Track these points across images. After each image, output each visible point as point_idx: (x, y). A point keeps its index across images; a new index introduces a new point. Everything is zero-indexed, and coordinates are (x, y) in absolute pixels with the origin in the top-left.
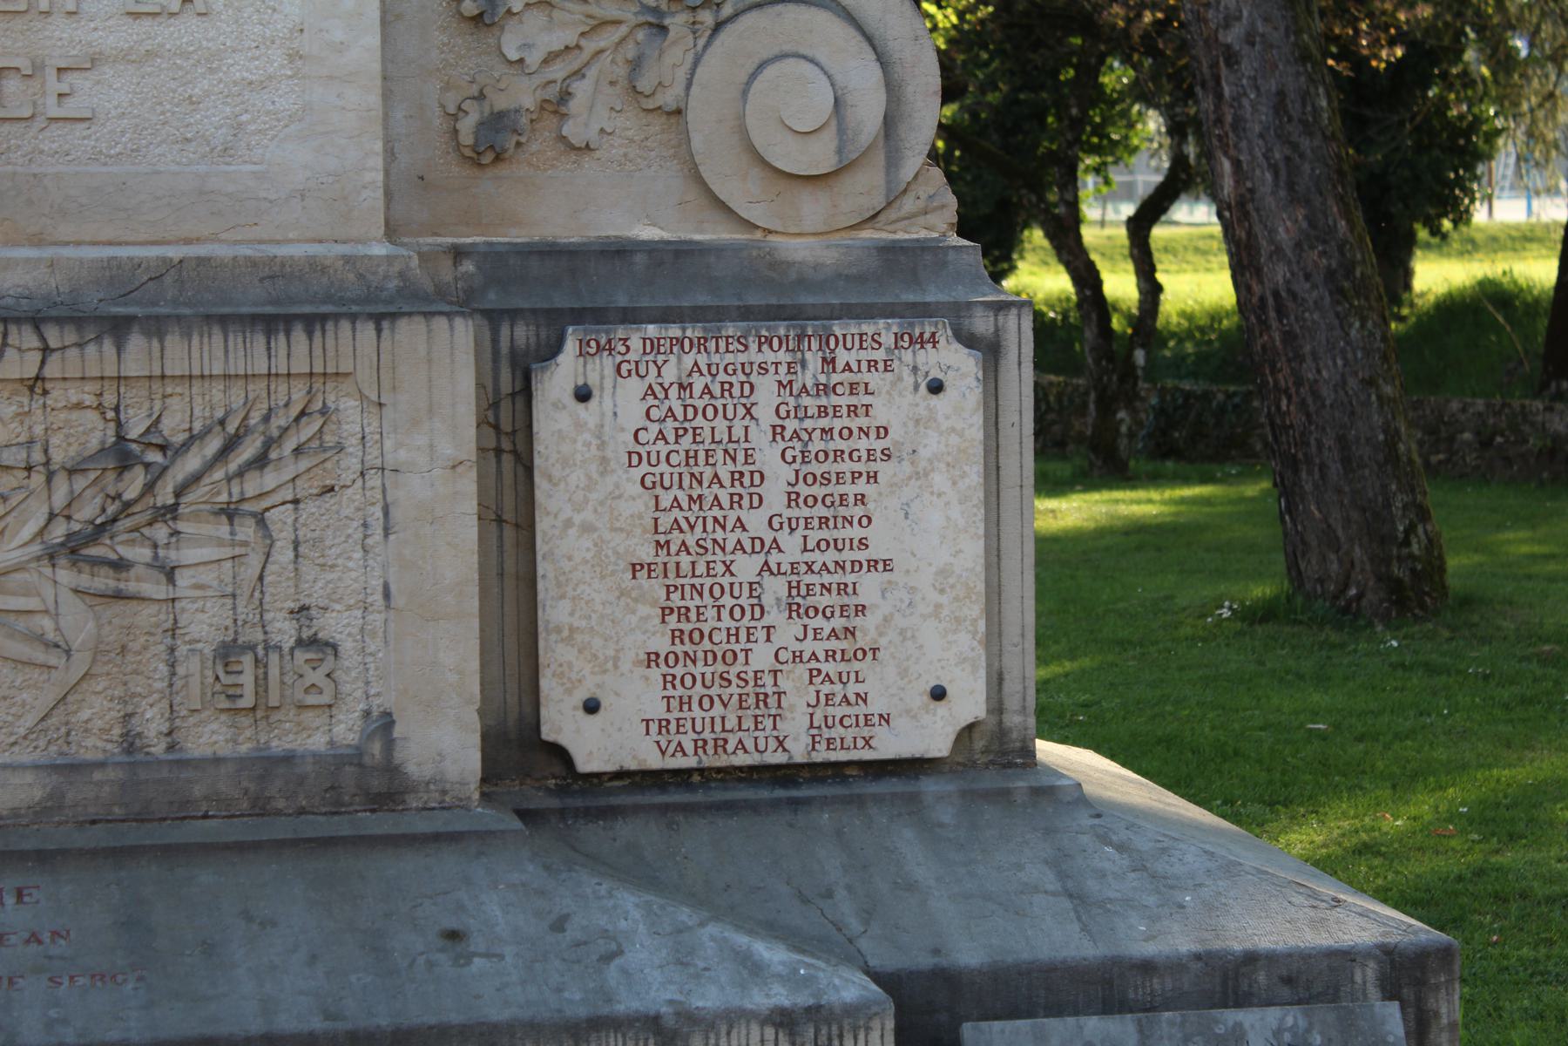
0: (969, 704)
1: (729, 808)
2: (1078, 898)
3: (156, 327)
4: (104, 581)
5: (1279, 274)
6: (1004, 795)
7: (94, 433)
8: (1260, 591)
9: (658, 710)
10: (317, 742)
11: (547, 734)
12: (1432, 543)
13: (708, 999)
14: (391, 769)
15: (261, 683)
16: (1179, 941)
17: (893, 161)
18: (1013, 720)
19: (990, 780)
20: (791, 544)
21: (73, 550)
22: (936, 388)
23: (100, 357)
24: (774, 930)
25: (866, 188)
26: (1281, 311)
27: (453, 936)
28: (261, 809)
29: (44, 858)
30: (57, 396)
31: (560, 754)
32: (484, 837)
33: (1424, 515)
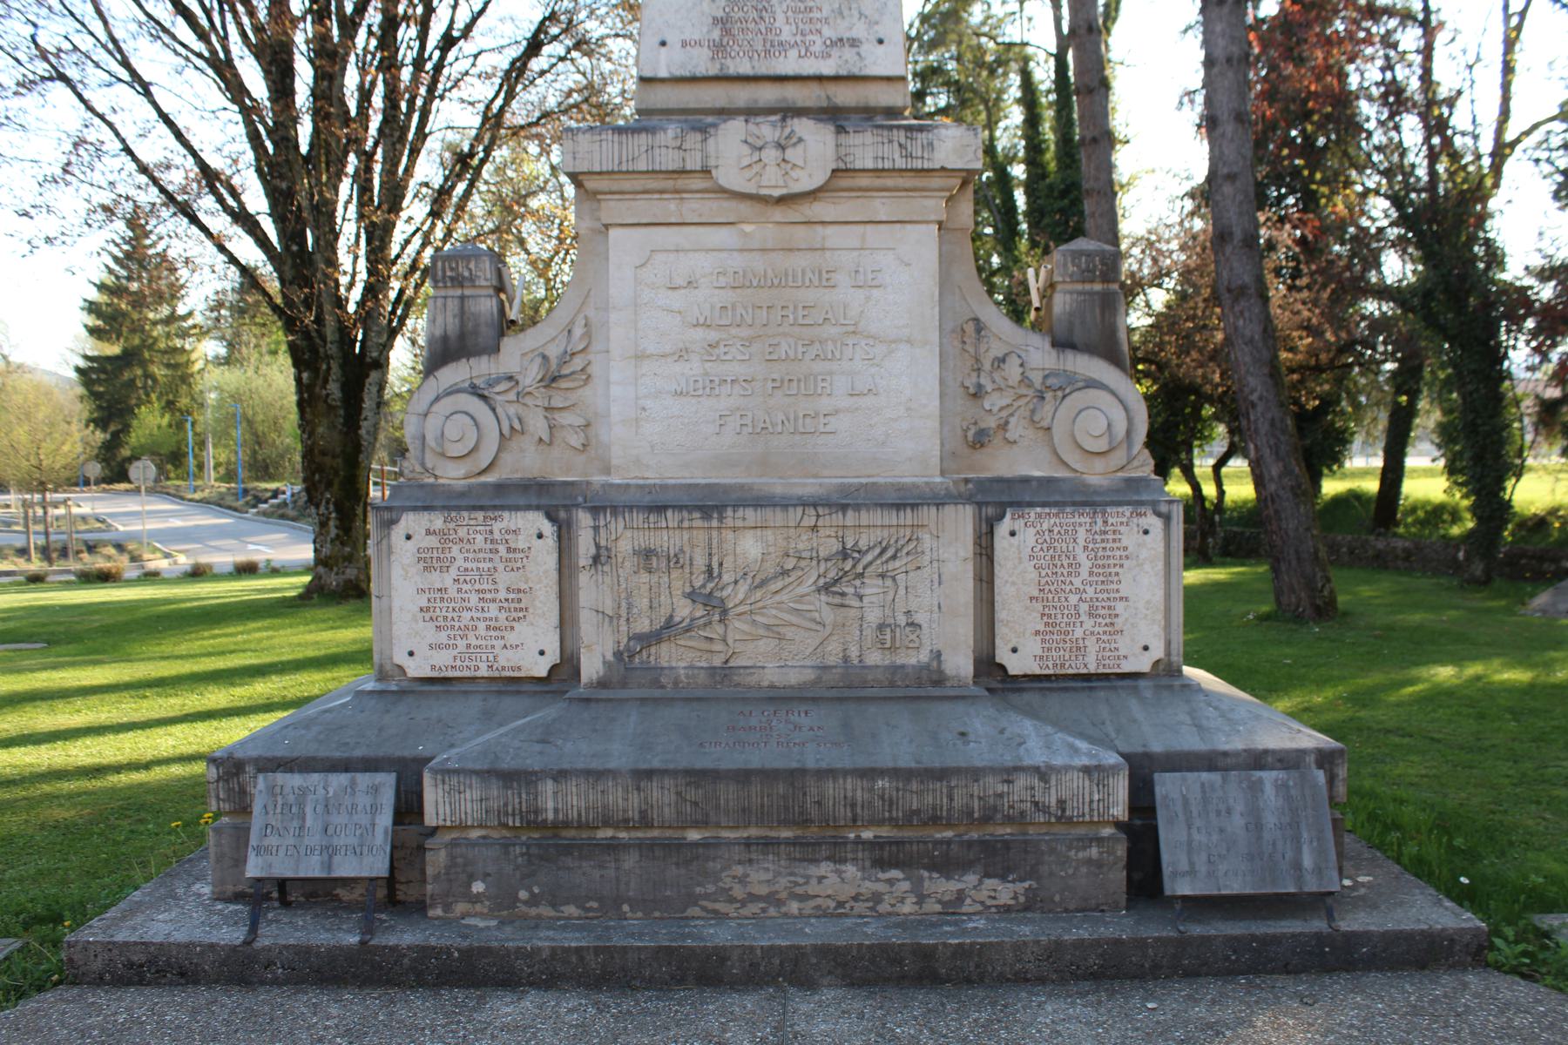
0: (1158, 652)
1: (1066, 689)
2: (1199, 727)
3: (857, 507)
4: (837, 600)
5: (1272, 487)
6: (1170, 687)
7: (835, 546)
8: (1265, 608)
9: (1039, 652)
10: (913, 661)
11: (998, 660)
12: (1332, 592)
13: (1058, 761)
14: (940, 672)
15: (893, 638)
16: (1237, 744)
17: (1130, 447)
18: (1174, 658)
19: (1165, 681)
20: (1090, 590)
21: (826, 588)
22: (1146, 532)
23: (838, 518)
24: (1082, 736)
25: (1119, 458)
26: (1273, 501)
27: (963, 734)
28: (892, 685)
29: (815, 700)
30: (822, 532)
31: (1002, 668)
32: (974, 698)
33: (1328, 580)
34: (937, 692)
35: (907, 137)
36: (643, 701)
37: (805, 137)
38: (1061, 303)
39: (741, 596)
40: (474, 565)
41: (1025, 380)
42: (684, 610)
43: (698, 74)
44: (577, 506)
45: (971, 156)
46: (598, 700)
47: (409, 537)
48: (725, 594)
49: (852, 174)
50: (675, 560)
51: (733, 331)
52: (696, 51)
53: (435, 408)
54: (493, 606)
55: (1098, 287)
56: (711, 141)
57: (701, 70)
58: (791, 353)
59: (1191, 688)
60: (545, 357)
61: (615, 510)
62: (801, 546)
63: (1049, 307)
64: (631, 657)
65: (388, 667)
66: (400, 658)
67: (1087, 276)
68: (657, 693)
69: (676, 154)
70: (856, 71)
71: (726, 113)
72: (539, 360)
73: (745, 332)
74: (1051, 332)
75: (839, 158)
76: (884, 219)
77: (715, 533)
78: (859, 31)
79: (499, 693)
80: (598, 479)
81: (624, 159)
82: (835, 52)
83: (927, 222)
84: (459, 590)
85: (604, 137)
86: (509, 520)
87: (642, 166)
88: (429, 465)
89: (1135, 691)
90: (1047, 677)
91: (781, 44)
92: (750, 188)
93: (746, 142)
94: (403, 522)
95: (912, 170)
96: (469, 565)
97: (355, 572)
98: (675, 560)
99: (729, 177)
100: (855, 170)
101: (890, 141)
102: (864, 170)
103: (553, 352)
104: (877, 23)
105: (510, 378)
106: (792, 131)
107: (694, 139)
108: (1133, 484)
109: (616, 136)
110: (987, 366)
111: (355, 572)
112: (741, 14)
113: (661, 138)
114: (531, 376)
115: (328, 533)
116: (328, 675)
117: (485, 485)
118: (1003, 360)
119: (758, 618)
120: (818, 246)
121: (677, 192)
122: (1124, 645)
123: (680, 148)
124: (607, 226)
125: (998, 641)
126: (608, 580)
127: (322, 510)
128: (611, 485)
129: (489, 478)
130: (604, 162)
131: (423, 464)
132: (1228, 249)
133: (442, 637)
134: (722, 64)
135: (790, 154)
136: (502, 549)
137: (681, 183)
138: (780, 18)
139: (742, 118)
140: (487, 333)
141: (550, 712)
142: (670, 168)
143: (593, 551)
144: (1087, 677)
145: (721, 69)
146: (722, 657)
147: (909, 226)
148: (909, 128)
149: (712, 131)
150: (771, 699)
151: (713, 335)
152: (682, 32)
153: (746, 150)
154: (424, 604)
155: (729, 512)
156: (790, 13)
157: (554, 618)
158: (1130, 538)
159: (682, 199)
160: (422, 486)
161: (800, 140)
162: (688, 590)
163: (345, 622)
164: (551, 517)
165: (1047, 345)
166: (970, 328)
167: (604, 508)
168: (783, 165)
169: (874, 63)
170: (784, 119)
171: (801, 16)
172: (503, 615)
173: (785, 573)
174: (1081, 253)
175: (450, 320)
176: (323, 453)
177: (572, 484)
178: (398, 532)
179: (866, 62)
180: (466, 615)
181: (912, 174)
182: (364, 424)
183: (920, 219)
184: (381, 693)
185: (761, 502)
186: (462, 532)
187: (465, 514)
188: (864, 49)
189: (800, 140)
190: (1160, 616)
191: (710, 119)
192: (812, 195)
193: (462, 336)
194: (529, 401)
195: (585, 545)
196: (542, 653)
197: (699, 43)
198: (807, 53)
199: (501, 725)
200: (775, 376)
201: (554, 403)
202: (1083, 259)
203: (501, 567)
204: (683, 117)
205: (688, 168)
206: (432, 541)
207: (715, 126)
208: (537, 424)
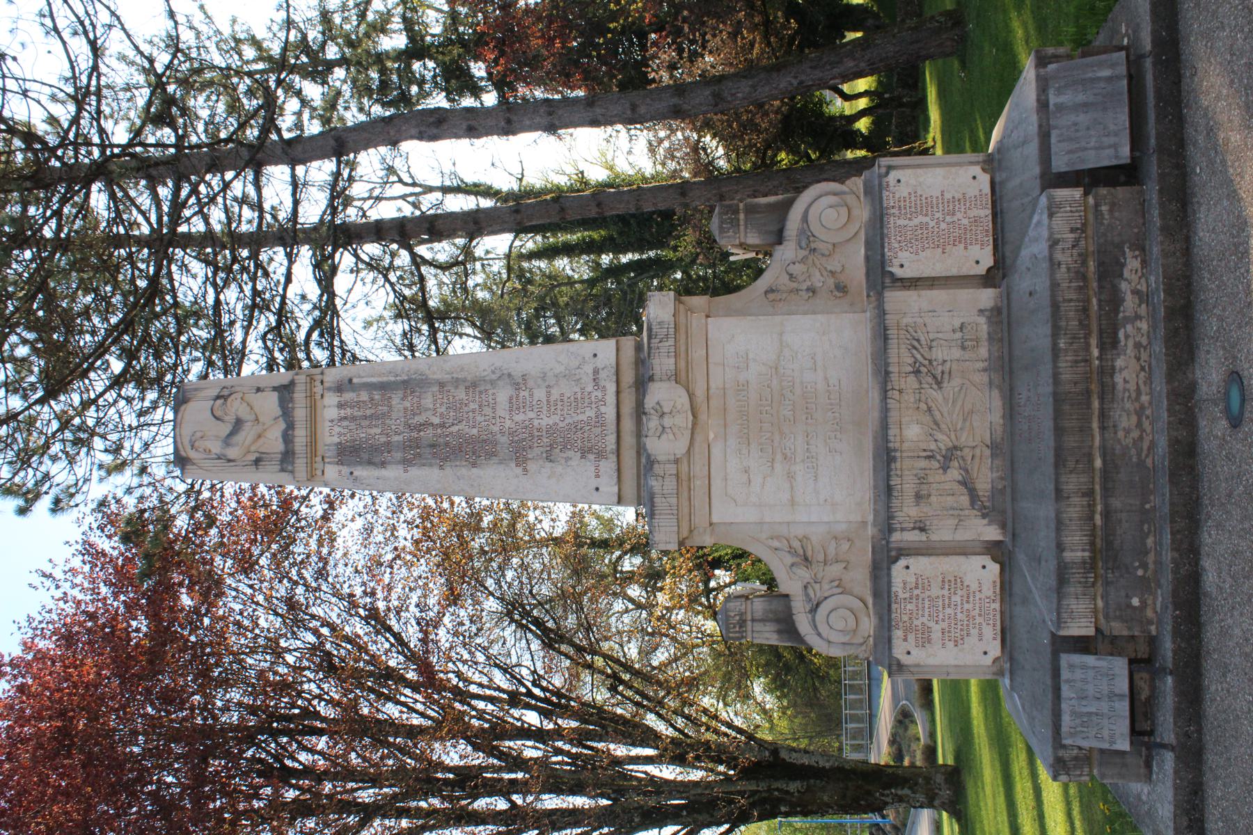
0: (977, 170)
1: (1002, 229)
2: (1024, 143)
3: (887, 364)
4: (946, 376)
5: (863, 65)
6: (1000, 161)
7: (912, 378)
8: (956, 64)
9: (978, 247)
10: (985, 327)
11: (984, 273)
12: (941, 14)
13: (1045, 234)
14: (992, 310)
15: (971, 340)
16: (1034, 118)
17: (844, 193)
18: (981, 159)
19: (996, 164)
20: (937, 215)
21: (939, 383)
22: (899, 181)
23: (894, 377)
24: (1031, 218)
25: (850, 199)
26: (873, 64)
27: (1031, 294)
28: (1001, 340)
29: (1011, 389)
30: (903, 386)
31: (989, 270)
32: (1008, 287)
33: (933, 17)
34: (1005, 312)
36: (1013, 499)
38: (753, 239)
39: (945, 438)
40: (927, 610)
41: (803, 261)
42: (954, 473)
44: (888, 542)
46: (1014, 529)
47: (909, 653)
48: (943, 447)
50: (922, 480)
51: (776, 444)
52: (602, 469)
53: (824, 635)
54: (953, 599)
55: (742, 216)
56: (659, 458)
57: (614, 466)
58: (790, 408)
59: (1000, 148)
60: (793, 565)
61: (890, 517)
62: (912, 400)
63: (757, 246)
64: (985, 508)
65: (995, 669)
66: (988, 660)
67: (735, 224)
68: (1009, 490)
69: (667, 480)
70: (613, 370)
71: (640, 449)
72: (794, 569)
73: (777, 437)
74: (773, 245)
77: (905, 454)
78: (589, 369)
79: (1011, 595)
80: (870, 531)
82: (602, 383)
84: (943, 620)
86: (897, 586)
88: (861, 641)
89: (1002, 183)
90: (995, 240)
92: (688, 434)
94: (899, 657)
96: (926, 614)
97: (939, 776)
98: (922, 480)
99: (680, 447)
103: (789, 560)
105: (806, 587)
107: (658, 469)
108: (868, 190)
110: (795, 285)
111: (939, 776)
114: (804, 574)
115: (907, 796)
116: (1018, 778)
117: (874, 604)
118: (791, 275)
119: (959, 427)
122: (972, 191)
124: (711, 524)
125: (972, 273)
126: (935, 522)
127: (889, 800)
128: (875, 520)
129: (870, 601)
131: (862, 644)
132: (686, 107)
133: (974, 632)
135: (666, 410)
136: (916, 592)
137: (684, 476)
138: (581, 417)
140: (777, 605)
141: (1021, 558)
143: (917, 532)
144: (994, 215)
146: (985, 449)
147: (710, 336)
148: (650, 337)
150: (1011, 417)
151: (779, 457)
153: (664, 436)
154: (952, 644)
155: (891, 445)
157: (962, 559)
158: (903, 191)
160: (875, 645)
161: (658, 403)
162: (941, 471)
163: (979, 777)
164: (896, 560)
165: (781, 247)
166: (771, 296)
167: (889, 525)
170: (645, 414)
172: (959, 592)
173: (929, 409)
175: (767, 628)
176: (844, 797)
177: (873, 548)
178: (905, 660)
180: (959, 616)
182: (821, 764)
184: (1011, 673)
185: (884, 425)
186: (905, 618)
187: (893, 616)
188: (600, 366)
189: (658, 403)
190: (953, 170)
191: (643, 460)
192: (691, 396)
193: (778, 621)
194: (819, 576)
195: (913, 537)
196: (984, 567)
197: (597, 467)
198: (603, 400)
199: (1031, 592)
200: (804, 417)
201: (821, 558)
203: (928, 593)
206: (911, 637)
207: (649, 456)
208: (835, 570)
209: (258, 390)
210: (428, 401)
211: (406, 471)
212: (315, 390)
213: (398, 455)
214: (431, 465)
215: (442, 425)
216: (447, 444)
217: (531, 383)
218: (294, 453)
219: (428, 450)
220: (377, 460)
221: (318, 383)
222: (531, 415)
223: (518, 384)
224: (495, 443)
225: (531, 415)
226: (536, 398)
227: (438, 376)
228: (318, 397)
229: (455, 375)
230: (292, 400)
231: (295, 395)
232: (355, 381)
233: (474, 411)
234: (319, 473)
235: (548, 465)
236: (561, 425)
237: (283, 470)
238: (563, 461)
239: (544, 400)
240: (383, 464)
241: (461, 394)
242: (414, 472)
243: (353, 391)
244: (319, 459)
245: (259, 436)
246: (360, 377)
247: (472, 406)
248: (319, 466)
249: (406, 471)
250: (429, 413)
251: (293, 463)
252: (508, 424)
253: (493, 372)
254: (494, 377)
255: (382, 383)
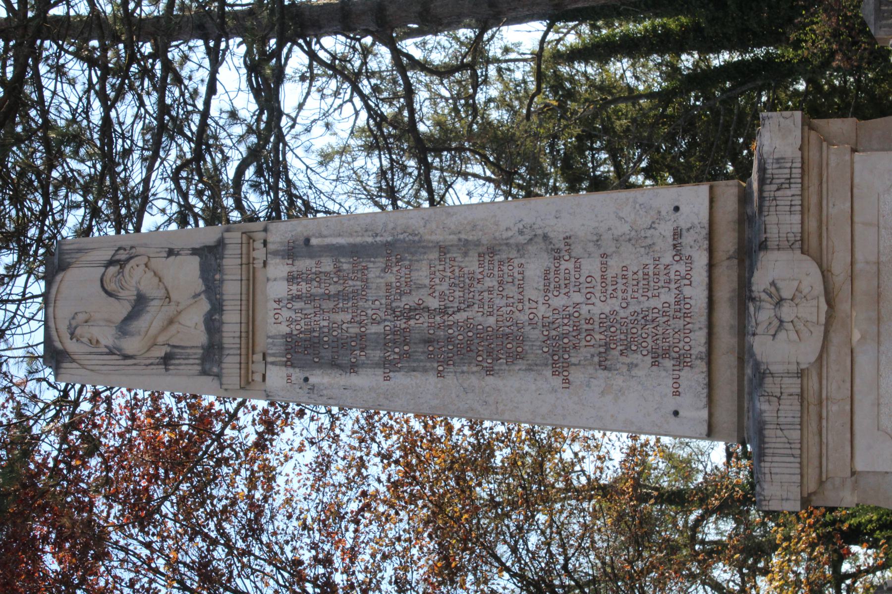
35: (771, 183)
37: (771, 281)
43: (706, 381)
45: (789, 122)
49: (806, 236)
52: (684, 383)
56: (773, 368)
57: (702, 378)
69: (786, 401)
70: (705, 232)
71: (744, 354)
75: (791, 247)
76: (849, 204)
78: (666, 229)
81: (789, 452)
82: (686, 252)
83: (852, 162)
85: (767, 471)
87: (795, 435)
91: (677, 303)
92: (819, 332)
93: (774, 336)
95: (802, 178)
99: (807, 353)
100: (802, 233)
101: (775, 199)
102: (802, 223)
104: (659, 212)
106: (764, 291)
107: (770, 385)
109: (767, 459)
112: (649, 340)
113: (769, 416)
120: (875, 268)
121: (820, 403)
123: (779, 398)
124: (853, 473)
130: (792, 471)
134: (696, 358)
135: (786, 294)
137: (812, 398)
138: (653, 303)
139: (750, 339)
142: (799, 408)
145: (701, 359)
147: (857, 180)
148: (762, 181)
149: (763, 367)
152: (666, 395)
153: (782, 335)
156: (649, 294)
159: (827, 399)
161: (773, 284)
168: (797, 301)
169: (697, 215)
170: (753, 299)
171: (652, 284)
174: (878, 11)
179: (696, 222)
181: (806, 178)
183: (849, 170)
188: (684, 225)
189: (773, 284)
191: (749, 371)
192: (825, 273)
198: (688, 277)
202: (884, 8)
204: (746, 397)
205: (799, 390)
207: (757, 365)
209: (171, 253)
210: (422, 274)
211: (387, 378)
212: (255, 254)
213: (376, 354)
214: (425, 370)
215: (443, 311)
216: (449, 339)
217: (577, 250)
218: (221, 348)
219: (421, 348)
220: (344, 361)
221: (259, 245)
222: (577, 298)
223: (558, 250)
224: (522, 340)
225: (577, 298)
226: (585, 272)
227: (438, 237)
228: (259, 264)
229: (463, 236)
230: (219, 268)
231: (225, 262)
232: (314, 241)
233: (490, 291)
234: (258, 377)
235: (602, 374)
236: (622, 313)
237: (204, 373)
238: (624, 369)
239: (597, 276)
240: (353, 368)
241: (472, 264)
242: (401, 380)
243: (311, 256)
244: (258, 357)
245: (171, 322)
246: (321, 236)
247: (489, 283)
248: (259, 367)
249: (387, 378)
250: (425, 292)
251: (220, 363)
252: (542, 310)
253: (521, 232)
254: (522, 239)
255: (354, 246)
